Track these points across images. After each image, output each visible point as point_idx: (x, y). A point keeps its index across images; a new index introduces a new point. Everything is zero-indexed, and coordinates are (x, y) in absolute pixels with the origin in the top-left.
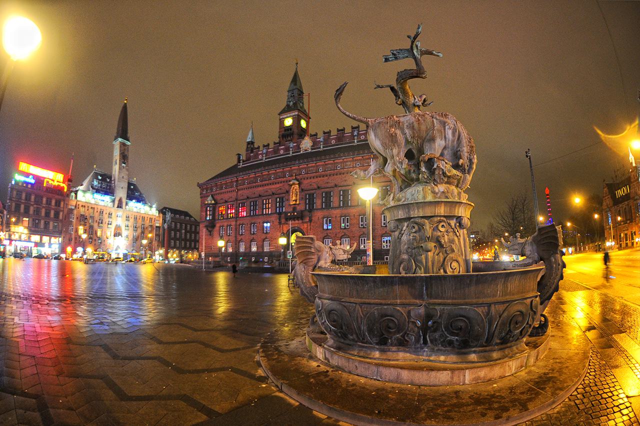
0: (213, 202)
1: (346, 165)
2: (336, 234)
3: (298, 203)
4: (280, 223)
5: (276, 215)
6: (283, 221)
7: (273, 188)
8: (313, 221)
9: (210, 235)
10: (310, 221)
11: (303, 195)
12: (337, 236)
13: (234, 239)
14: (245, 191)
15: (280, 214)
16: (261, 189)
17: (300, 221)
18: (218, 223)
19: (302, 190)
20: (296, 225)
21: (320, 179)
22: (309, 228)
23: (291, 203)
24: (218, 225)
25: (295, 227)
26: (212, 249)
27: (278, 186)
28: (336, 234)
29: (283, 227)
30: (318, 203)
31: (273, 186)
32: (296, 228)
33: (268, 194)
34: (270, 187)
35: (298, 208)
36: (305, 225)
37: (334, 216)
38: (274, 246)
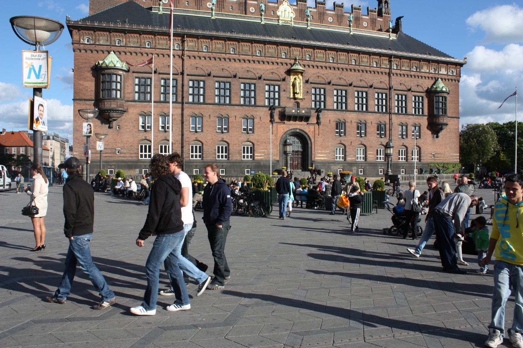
0: (125, 67)
2: (351, 142)
3: (301, 97)
4: (272, 121)
5: (265, 109)
6: (276, 118)
7: (260, 69)
8: (322, 123)
10: (318, 123)
11: (308, 89)
12: (352, 144)
14: (202, 63)
15: (272, 108)
16: (237, 65)
18: (134, 106)
19: (307, 82)
20: (298, 127)
21: (330, 71)
22: (317, 132)
25: (297, 129)
26: (115, 153)
28: (351, 142)
29: (277, 127)
30: (332, 102)
32: (298, 131)
33: (250, 75)
34: (252, 66)
35: (302, 104)
36: (312, 128)
37: (349, 121)
38: (264, 152)
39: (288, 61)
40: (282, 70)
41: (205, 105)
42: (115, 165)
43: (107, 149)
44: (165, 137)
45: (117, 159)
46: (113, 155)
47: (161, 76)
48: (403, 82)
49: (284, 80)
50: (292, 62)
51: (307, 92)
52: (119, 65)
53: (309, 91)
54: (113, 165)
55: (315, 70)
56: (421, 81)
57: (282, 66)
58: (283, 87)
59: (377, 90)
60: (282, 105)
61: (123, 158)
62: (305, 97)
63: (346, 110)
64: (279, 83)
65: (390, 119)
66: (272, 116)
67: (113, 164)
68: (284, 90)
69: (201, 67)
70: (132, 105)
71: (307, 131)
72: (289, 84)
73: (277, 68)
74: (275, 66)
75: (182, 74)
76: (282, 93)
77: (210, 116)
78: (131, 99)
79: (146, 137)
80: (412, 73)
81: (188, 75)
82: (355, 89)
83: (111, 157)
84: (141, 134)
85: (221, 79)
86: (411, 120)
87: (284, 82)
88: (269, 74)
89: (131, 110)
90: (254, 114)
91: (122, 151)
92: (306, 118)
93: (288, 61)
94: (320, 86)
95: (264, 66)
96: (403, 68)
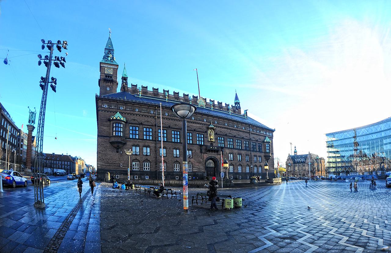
1: (239, 126)
3: (214, 141)
4: (201, 152)
5: (197, 146)
7: (194, 126)
9: (118, 152)
13: (154, 159)
17: (216, 153)
18: (130, 141)
20: (213, 155)
21: (226, 130)
23: (209, 140)
24: (129, 144)
27: (198, 125)
31: (194, 125)
37: (235, 153)
39: (207, 123)
40: (204, 128)
41: (167, 143)
42: (120, 173)
43: (115, 164)
44: (147, 159)
45: (121, 169)
46: (118, 167)
47: (144, 126)
48: (254, 137)
49: (206, 132)
50: (209, 124)
51: (216, 139)
52: (122, 119)
53: (217, 138)
54: (118, 173)
55: (219, 129)
56: (261, 137)
57: (204, 126)
58: (205, 135)
59: (245, 140)
60: (206, 144)
61: (124, 169)
62: (216, 141)
63: (233, 148)
64: (203, 133)
65: (251, 153)
66: (201, 150)
67: (118, 172)
68: (206, 137)
69: (165, 123)
70: (128, 140)
71: (217, 157)
72: (208, 134)
73: (202, 126)
74: (201, 126)
75: (155, 126)
76: (205, 139)
77: (170, 148)
78: (128, 137)
79: (136, 158)
80: (258, 133)
81: (158, 127)
82: (237, 138)
83: (118, 168)
84: (134, 156)
85: (175, 130)
86: (258, 154)
87: (206, 134)
88: (198, 128)
89: (128, 143)
90: (192, 148)
91: (123, 165)
92: (217, 151)
93: (207, 123)
94: (222, 136)
95: (196, 124)
96: (254, 131)
